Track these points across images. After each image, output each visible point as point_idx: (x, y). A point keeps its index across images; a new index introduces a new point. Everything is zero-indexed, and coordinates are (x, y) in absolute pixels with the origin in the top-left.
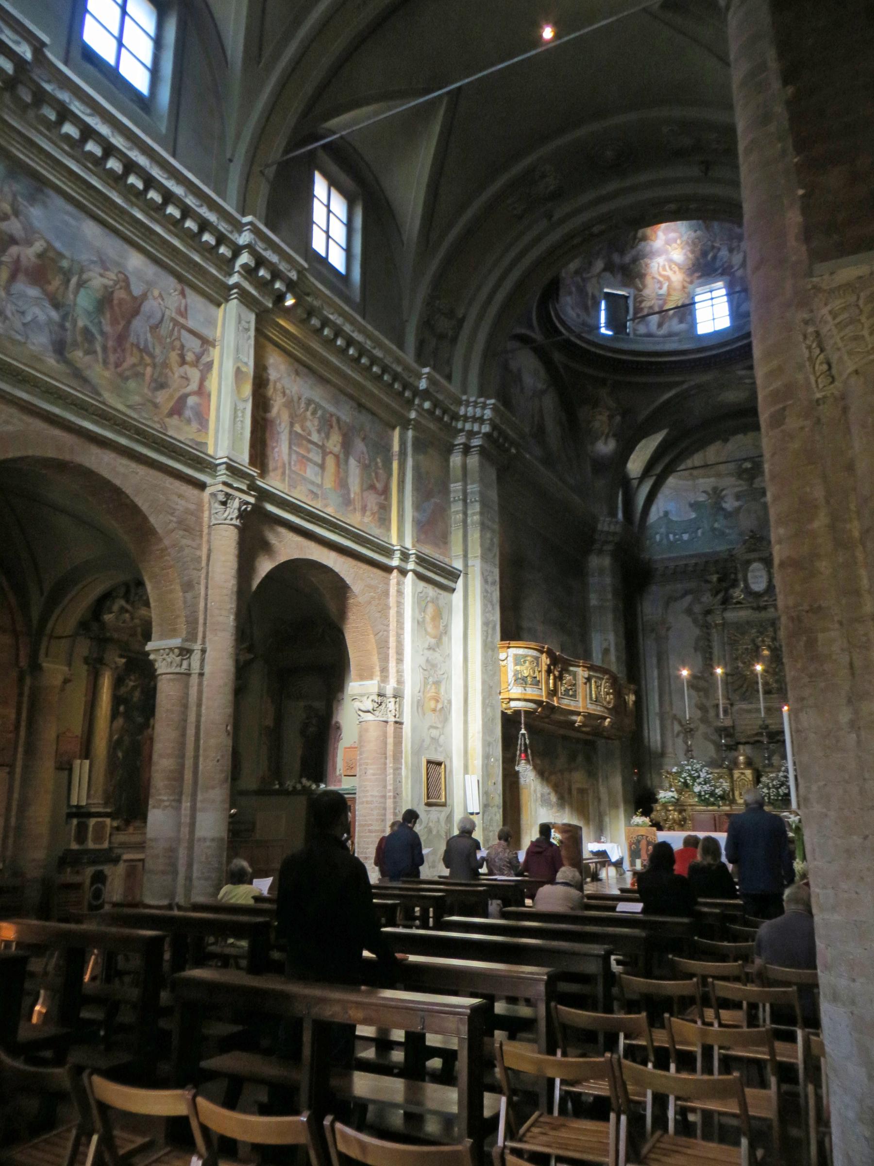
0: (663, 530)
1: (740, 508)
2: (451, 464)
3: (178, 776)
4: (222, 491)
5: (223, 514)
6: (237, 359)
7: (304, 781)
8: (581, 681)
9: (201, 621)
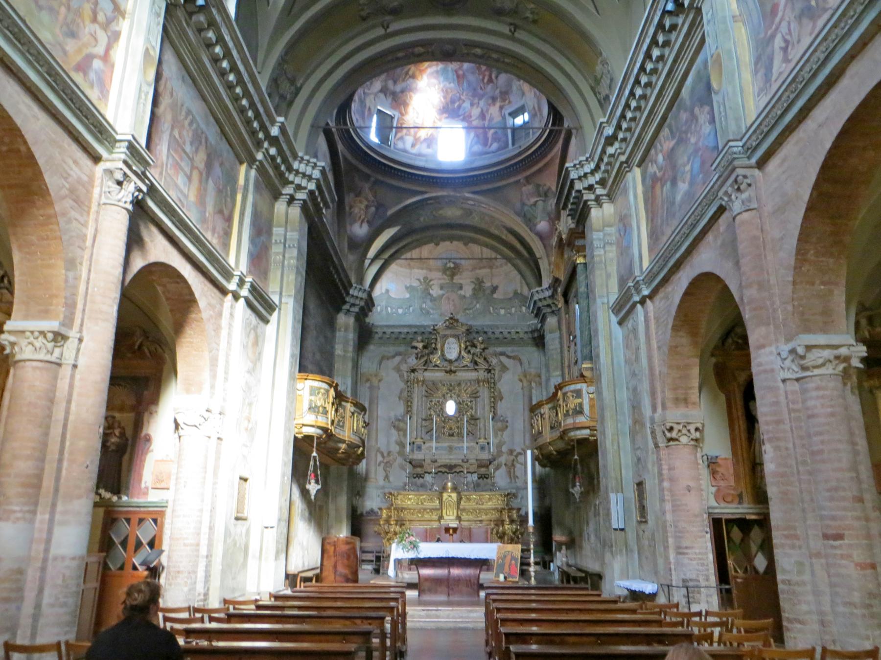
0: (384, 304)
1: (443, 295)
2: (276, 210)
3: (35, 484)
4: (121, 169)
5: (117, 194)
6: (148, 40)
7: (102, 491)
8: (348, 414)
9: (80, 306)
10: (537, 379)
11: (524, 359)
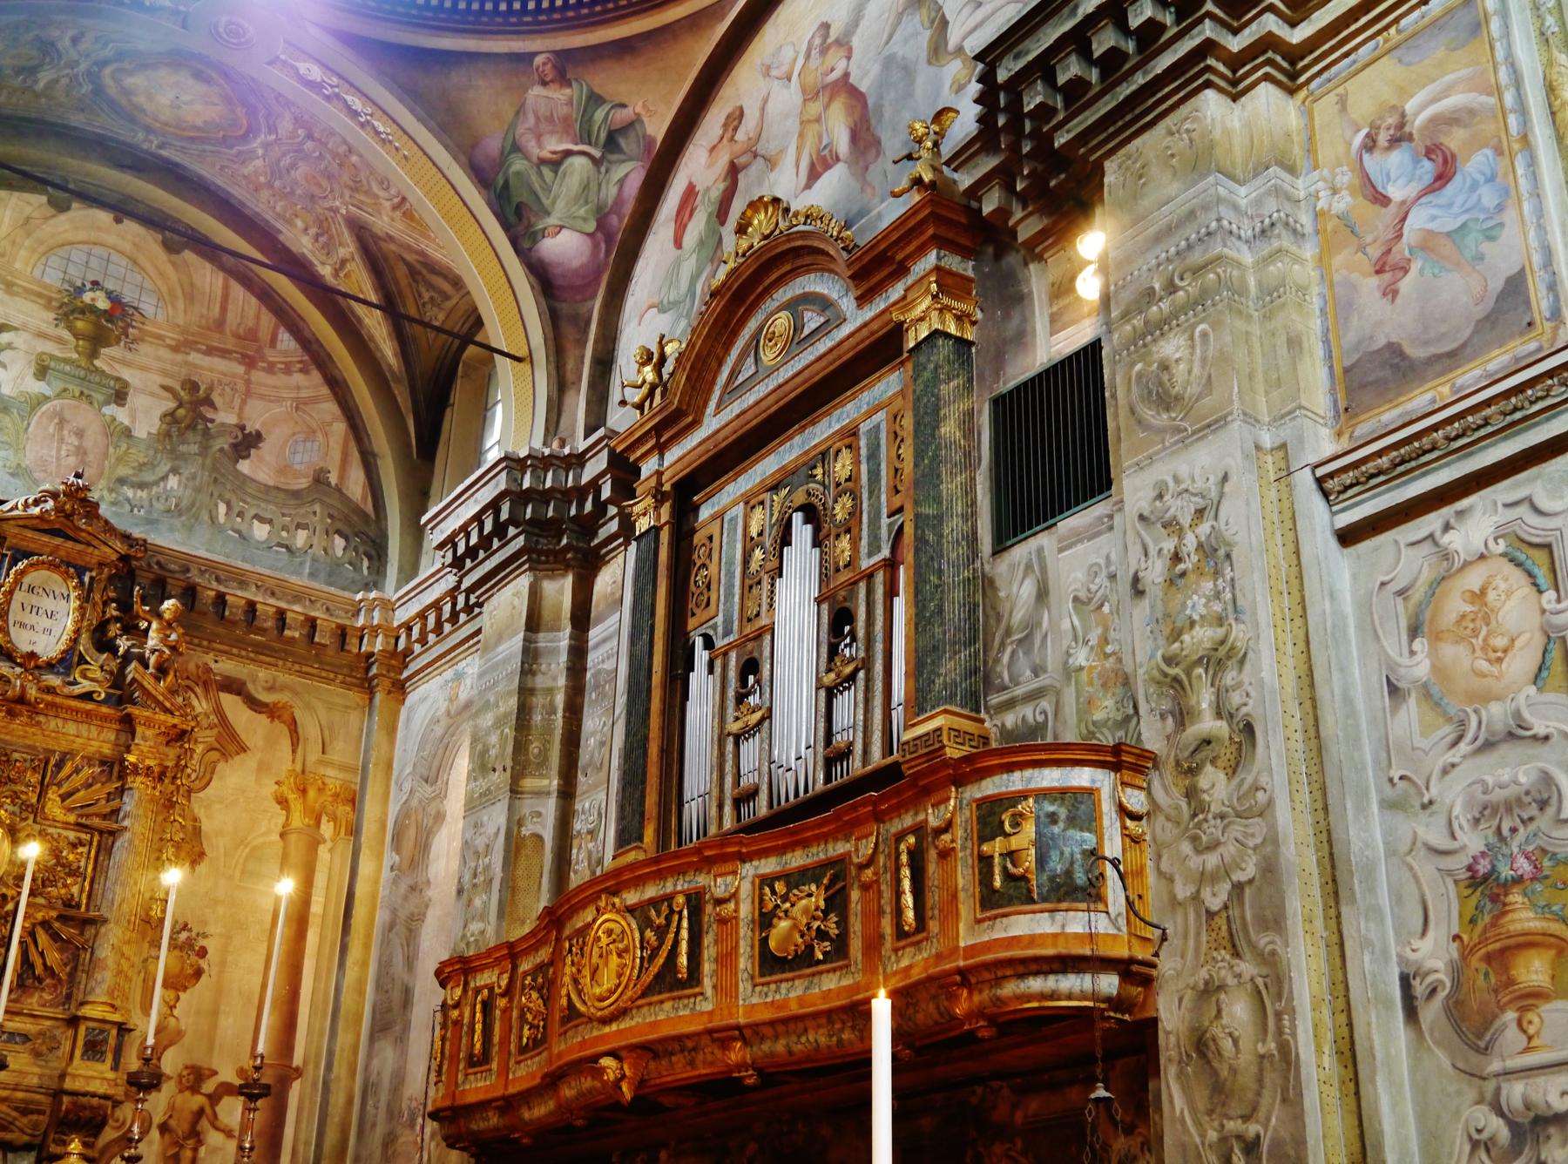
1: (47, 399)
10: (343, 810)
11: (310, 729)
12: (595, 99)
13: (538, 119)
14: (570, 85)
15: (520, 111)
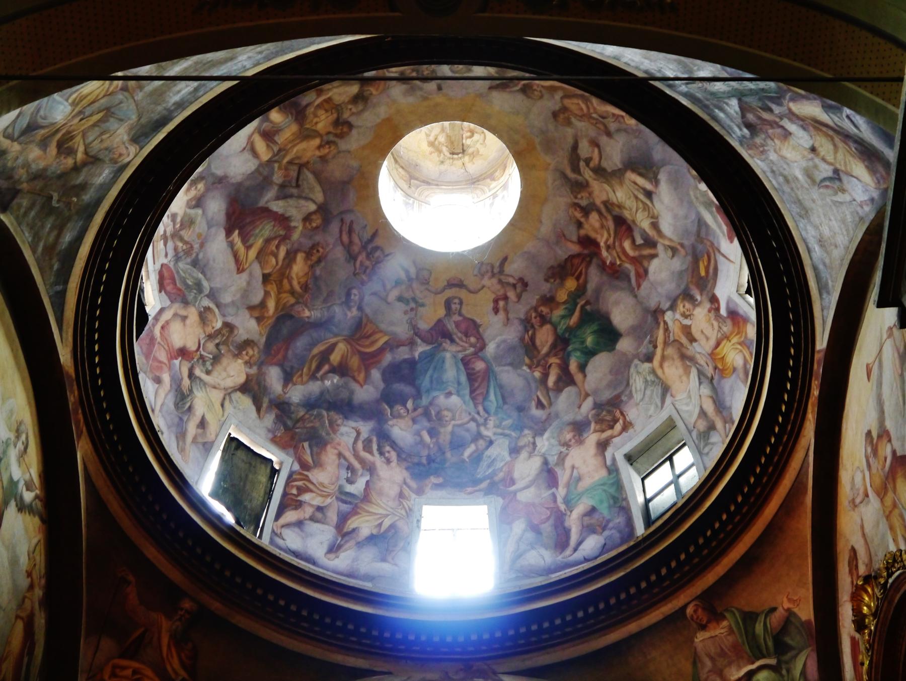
12: (749, 618)
13: (712, 659)
14: (724, 618)
15: (696, 660)
